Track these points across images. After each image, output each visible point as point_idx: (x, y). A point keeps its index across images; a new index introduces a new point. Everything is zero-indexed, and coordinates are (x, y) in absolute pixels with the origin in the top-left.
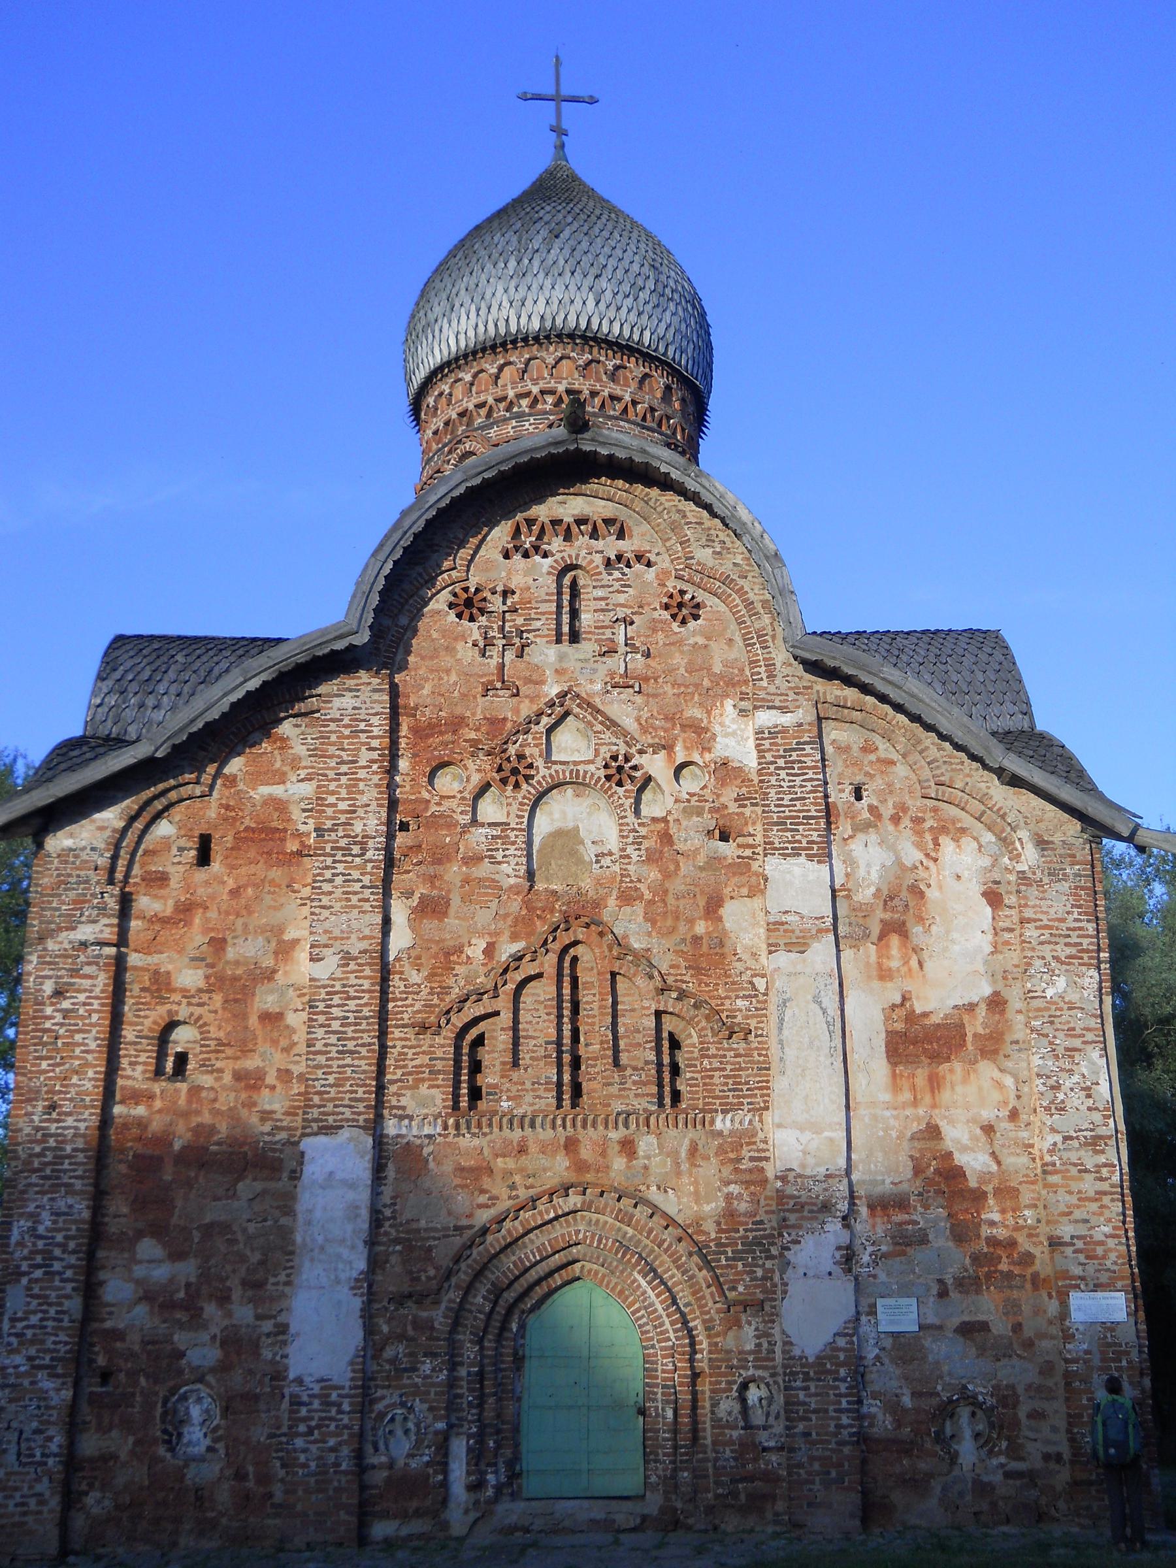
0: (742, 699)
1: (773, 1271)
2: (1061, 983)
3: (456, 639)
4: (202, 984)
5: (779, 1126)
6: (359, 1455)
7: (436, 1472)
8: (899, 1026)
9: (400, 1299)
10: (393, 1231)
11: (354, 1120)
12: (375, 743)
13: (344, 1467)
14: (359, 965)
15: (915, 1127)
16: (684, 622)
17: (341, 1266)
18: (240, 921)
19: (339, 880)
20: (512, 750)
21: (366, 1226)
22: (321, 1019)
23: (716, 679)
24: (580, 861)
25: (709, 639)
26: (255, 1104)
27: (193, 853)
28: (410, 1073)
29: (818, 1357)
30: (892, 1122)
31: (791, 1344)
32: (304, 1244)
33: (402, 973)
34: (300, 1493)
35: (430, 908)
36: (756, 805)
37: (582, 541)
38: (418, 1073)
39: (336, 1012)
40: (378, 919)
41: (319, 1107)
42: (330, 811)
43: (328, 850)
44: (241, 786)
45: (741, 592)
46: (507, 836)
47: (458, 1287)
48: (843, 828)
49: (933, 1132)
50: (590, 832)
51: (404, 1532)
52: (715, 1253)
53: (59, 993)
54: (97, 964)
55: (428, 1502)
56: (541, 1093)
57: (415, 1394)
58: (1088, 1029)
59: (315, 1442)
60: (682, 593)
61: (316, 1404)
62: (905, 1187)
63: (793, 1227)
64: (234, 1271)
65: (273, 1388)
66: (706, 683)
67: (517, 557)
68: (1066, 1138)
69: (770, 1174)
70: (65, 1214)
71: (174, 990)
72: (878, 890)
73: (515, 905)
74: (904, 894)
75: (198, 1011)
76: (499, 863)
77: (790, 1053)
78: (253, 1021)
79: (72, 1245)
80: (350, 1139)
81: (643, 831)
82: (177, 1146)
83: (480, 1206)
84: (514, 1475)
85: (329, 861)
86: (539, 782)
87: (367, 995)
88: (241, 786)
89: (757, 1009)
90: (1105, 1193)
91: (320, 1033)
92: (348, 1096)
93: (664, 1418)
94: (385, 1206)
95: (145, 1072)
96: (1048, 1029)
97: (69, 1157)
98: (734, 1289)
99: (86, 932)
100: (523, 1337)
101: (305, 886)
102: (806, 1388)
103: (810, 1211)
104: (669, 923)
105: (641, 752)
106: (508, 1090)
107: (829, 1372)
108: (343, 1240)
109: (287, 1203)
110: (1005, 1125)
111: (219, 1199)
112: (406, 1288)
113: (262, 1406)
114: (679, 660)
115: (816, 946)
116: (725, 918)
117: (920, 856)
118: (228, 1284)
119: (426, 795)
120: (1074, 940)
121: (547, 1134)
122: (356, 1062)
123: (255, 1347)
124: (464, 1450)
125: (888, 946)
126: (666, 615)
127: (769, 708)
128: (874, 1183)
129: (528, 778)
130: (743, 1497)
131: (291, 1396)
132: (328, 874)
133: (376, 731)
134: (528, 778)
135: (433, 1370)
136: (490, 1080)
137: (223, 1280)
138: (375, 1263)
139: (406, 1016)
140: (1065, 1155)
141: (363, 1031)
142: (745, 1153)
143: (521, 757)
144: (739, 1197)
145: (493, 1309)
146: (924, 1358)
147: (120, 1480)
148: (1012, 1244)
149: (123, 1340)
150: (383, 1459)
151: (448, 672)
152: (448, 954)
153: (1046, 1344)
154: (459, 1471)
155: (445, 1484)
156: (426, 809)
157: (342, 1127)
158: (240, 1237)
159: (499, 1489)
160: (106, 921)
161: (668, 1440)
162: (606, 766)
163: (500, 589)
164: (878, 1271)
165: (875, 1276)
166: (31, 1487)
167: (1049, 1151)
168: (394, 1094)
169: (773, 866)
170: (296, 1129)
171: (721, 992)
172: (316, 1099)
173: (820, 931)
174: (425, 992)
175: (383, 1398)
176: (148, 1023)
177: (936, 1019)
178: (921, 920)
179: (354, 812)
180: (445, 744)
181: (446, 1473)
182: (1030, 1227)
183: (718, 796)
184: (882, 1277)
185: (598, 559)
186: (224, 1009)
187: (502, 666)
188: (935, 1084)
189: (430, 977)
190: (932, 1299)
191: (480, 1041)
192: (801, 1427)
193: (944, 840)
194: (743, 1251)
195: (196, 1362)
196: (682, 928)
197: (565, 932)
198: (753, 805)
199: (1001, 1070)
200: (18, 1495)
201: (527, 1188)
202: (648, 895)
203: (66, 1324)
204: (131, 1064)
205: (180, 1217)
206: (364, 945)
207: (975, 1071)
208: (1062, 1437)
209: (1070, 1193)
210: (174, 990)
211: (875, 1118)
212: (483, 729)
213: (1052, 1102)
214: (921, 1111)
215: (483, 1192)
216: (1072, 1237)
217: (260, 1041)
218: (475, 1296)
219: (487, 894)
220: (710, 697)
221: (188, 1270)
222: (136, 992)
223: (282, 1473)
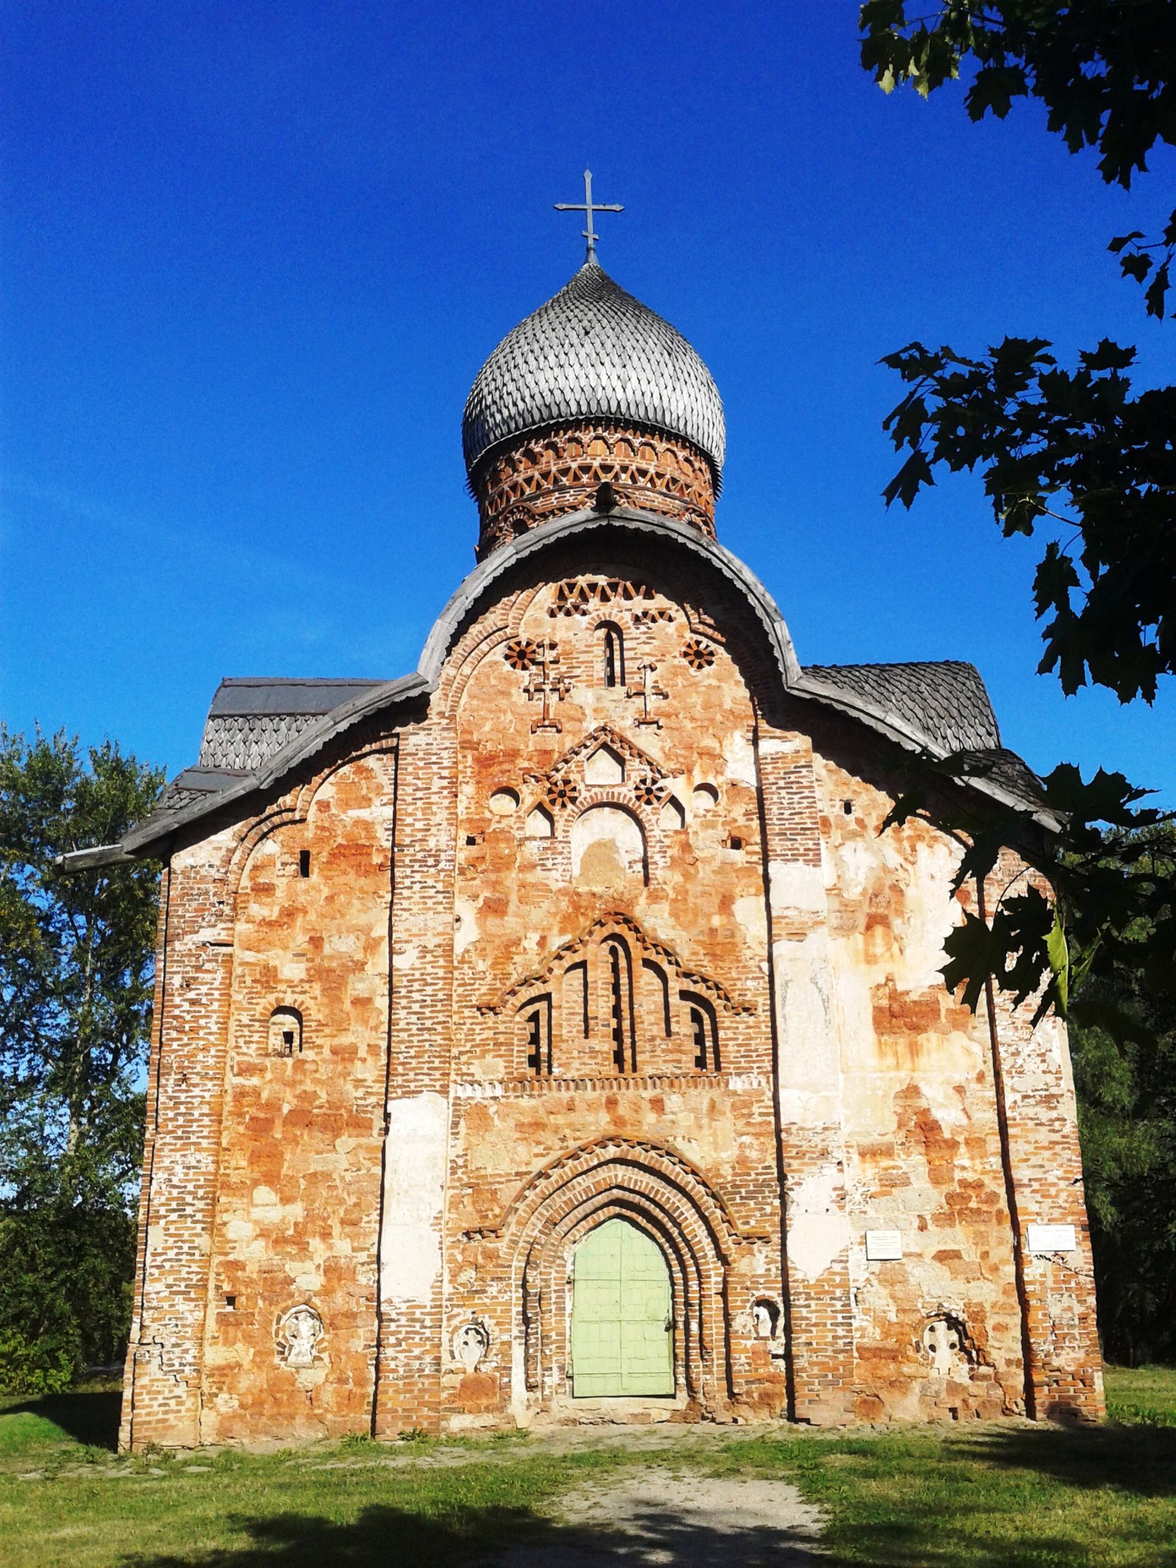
4: (304, 976)
8: (885, 1003)
10: (465, 1177)
12: (445, 773)
13: (427, 1372)
15: (898, 1088)
16: (700, 667)
19: (417, 887)
20: (558, 777)
22: (404, 1002)
24: (616, 867)
25: (720, 680)
27: (294, 867)
30: (879, 1083)
34: (391, 1393)
35: (494, 908)
39: (416, 996)
40: (450, 918)
42: (408, 830)
43: (407, 862)
44: (334, 810)
48: (836, 836)
49: (912, 1091)
51: (477, 1425)
53: (187, 985)
56: (586, 1060)
59: (404, 1351)
61: (403, 1320)
62: (890, 1138)
66: (719, 718)
67: (561, 615)
71: (281, 981)
72: (865, 890)
73: (564, 904)
74: (887, 891)
75: (300, 998)
81: (667, 842)
82: (286, 1109)
83: (536, 1155)
85: (408, 871)
98: (747, 1223)
99: (207, 935)
102: (808, 1306)
105: (663, 777)
107: (826, 1292)
112: (477, 1224)
113: (359, 1322)
114: (696, 699)
115: (812, 936)
117: (901, 860)
119: (488, 815)
121: (590, 1094)
125: (873, 936)
129: (573, 800)
130: (756, 1395)
132: (407, 882)
134: (573, 800)
139: (474, 998)
140: (1024, 1111)
143: (567, 782)
144: (751, 1146)
146: (905, 1282)
147: (244, 1383)
148: (979, 1185)
149: (244, 1269)
150: (459, 1365)
151: (505, 712)
152: (507, 946)
158: (338, 1182)
160: (224, 925)
162: (637, 788)
163: (547, 642)
166: (171, 1391)
171: (734, 975)
172: (400, 1069)
173: (816, 923)
174: (489, 978)
176: (259, 1008)
177: (914, 996)
178: (900, 913)
180: (503, 772)
181: (509, 1375)
185: (627, 617)
186: (323, 995)
187: (546, 708)
188: (914, 1050)
189: (494, 965)
191: (534, 1018)
192: (803, 1338)
193: (921, 847)
196: (702, 922)
200: (160, 1397)
201: (575, 1139)
202: (672, 895)
203: (197, 1257)
209: (1028, 1142)
210: (281, 981)
215: (538, 1143)
221: (296, 1211)
222: (248, 980)
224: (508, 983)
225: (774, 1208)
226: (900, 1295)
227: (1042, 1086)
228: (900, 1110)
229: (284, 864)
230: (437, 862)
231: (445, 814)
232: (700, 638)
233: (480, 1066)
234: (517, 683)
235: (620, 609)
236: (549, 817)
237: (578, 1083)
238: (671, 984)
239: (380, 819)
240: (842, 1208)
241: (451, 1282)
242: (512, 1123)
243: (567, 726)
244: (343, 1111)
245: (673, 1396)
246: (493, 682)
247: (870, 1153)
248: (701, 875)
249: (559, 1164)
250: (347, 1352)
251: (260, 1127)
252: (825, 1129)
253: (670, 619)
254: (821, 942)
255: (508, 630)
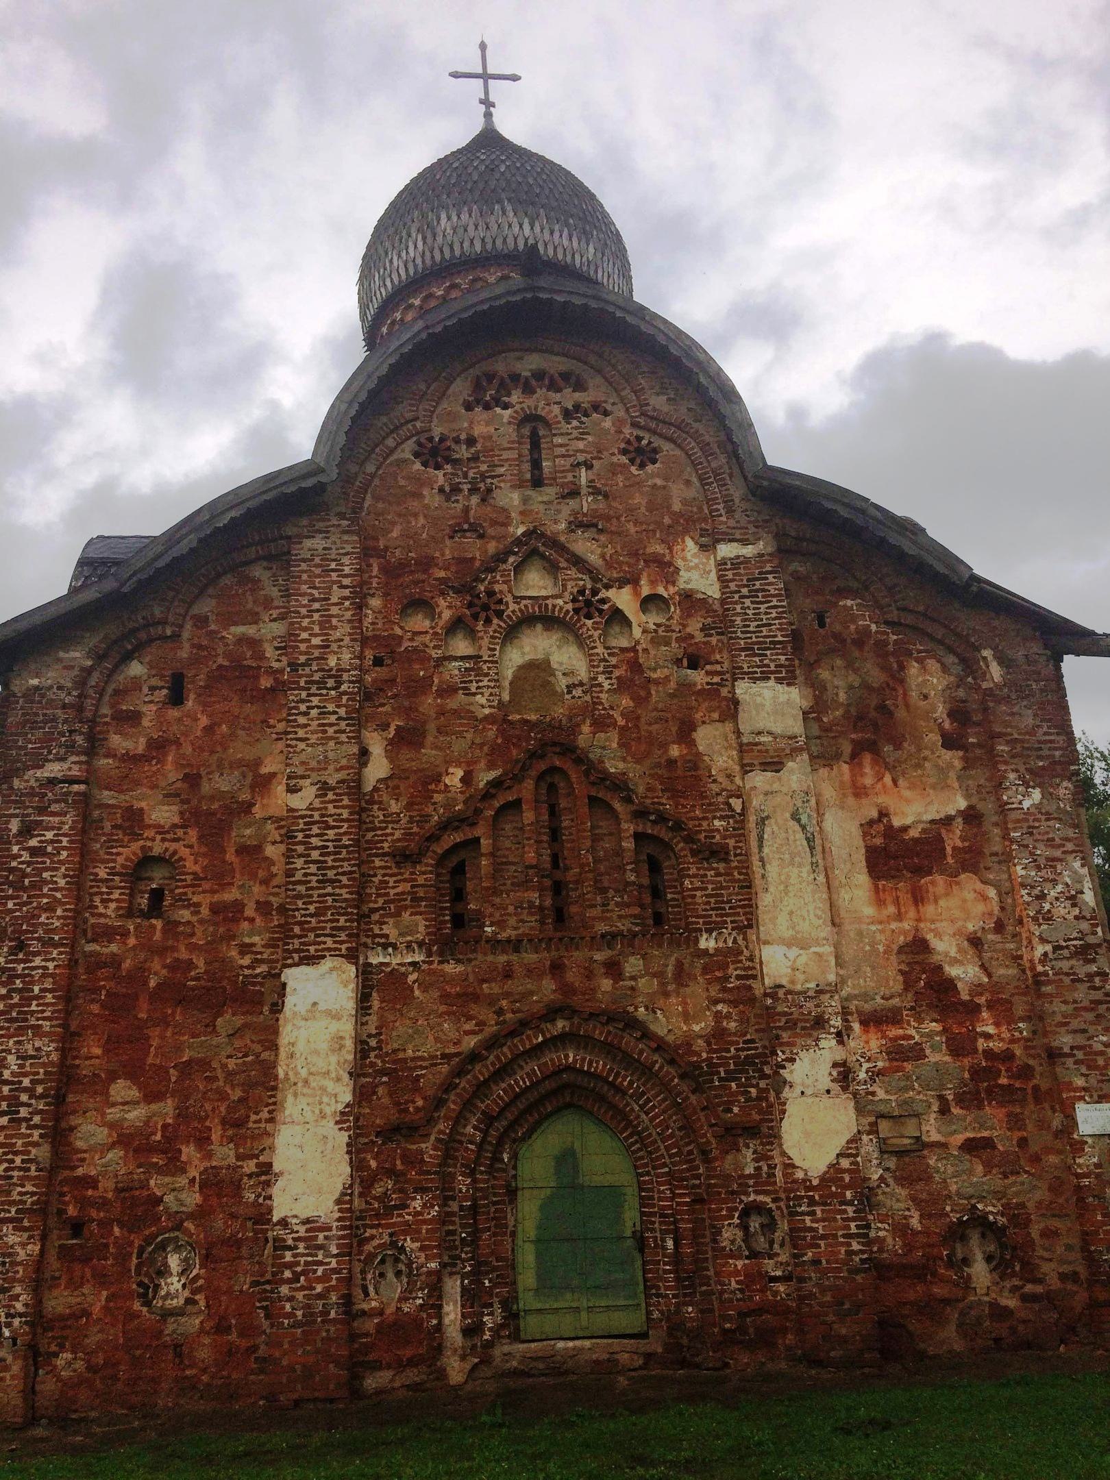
0: (702, 536)
1: (766, 1090)
2: (1036, 795)
3: (422, 485)
4: (176, 820)
5: (766, 943)
6: (348, 1300)
7: (430, 1317)
8: (878, 841)
9: (391, 1132)
10: (379, 1062)
11: (335, 949)
12: (346, 582)
14: (337, 794)
16: (642, 466)
17: (325, 1099)
18: (215, 757)
19: (314, 712)
21: (351, 1057)
22: (300, 849)
23: (677, 516)
25: (666, 479)
26: (233, 937)
27: (165, 692)
28: (392, 901)
29: (823, 1178)
30: (879, 937)
31: (793, 1166)
32: (287, 1078)
33: (381, 803)
35: (406, 739)
36: (722, 634)
37: (540, 392)
38: (400, 900)
40: (355, 749)
41: (300, 937)
42: (303, 647)
43: (302, 684)
45: (696, 436)
46: (480, 668)
47: (447, 1118)
49: (918, 946)
50: (561, 664)
52: (707, 1073)
54: (66, 801)
55: (422, 1351)
57: (405, 1233)
58: (1068, 839)
59: (302, 1288)
60: (639, 439)
62: (896, 1001)
63: (789, 1044)
64: (213, 1110)
65: (256, 1232)
68: (1057, 948)
69: (758, 992)
70: (32, 1057)
71: (149, 826)
72: (847, 712)
73: (492, 731)
74: (873, 714)
75: (173, 846)
76: (474, 694)
77: (773, 870)
78: (230, 856)
79: (40, 1089)
80: (332, 970)
81: (614, 660)
83: (467, 1033)
84: (512, 1316)
85: (304, 694)
86: (509, 616)
87: (346, 825)
88: (213, 627)
89: (734, 829)
90: (1099, 1002)
91: (299, 863)
92: (329, 925)
93: (664, 1248)
94: (370, 1036)
95: (118, 908)
96: (1028, 840)
97: (37, 998)
99: (54, 769)
100: (515, 1168)
101: (279, 721)
102: (813, 1213)
103: (803, 1028)
104: (643, 747)
105: (607, 587)
106: (491, 915)
107: (833, 1195)
108: (328, 1072)
109: (269, 1037)
110: (991, 937)
111: (198, 1036)
113: (245, 1251)
114: (639, 500)
116: (698, 741)
118: (207, 1124)
119: (398, 631)
120: (1045, 752)
121: (530, 957)
122: (338, 891)
123: (237, 1188)
124: (459, 1290)
125: (860, 765)
126: (624, 459)
127: (731, 541)
128: (866, 997)
129: (499, 614)
130: (751, 1330)
131: (275, 1240)
132: (303, 708)
133: (347, 570)
134: (499, 614)
135: (424, 1206)
136: (472, 906)
137: (202, 1120)
138: (363, 1094)
141: (343, 860)
142: (733, 972)
143: (490, 593)
144: (728, 1016)
145: (483, 1140)
148: (1008, 1056)
150: (374, 1304)
151: (416, 515)
153: (1053, 1159)
154: (452, 1313)
155: (439, 1328)
156: (400, 645)
157: (324, 957)
158: (219, 1073)
159: (496, 1331)
160: (74, 758)
161: (669, 1272)
162: (574, 600)
163: (463, 436)
164: (875, 1088)
165: (873, 1094)
167: (1040, 961)
168: (377, 922)
169: (743, 689)
170: (277, 961)
172: (297, 930)
175: (373, 1237)
176: (120, 860)
177: (914, 833)
179: (328, 647)
181: (440, 1317)
182: (1027, 1040)
183: (684, 626)
184: (881, 1094)
185: (556, 410)
187: (466, 510)
188: (918, 898)
189: (409, 806)
190: (933, 1116)
191: (459, 870)
194: (735, 1071)
195: (174, 1208)
197: (543, 756)
198: (718, 634)
199: (982, 882)
201: (514, 1012)
202: (621, 722)
204: (103, 901)
205: (156, 1055)
206: (342, 775)
207: (958, 883)
208: (1076, 1255)
211: (860, 933)
212: (453, 569)
213: (1038, 912)
214: (906, 925)
216: (1072, 1048)
217: (238, 876)
218: (465, 1126)
219: (461, 725)
220: (671, 535)
222: (108, 826)
223: (265, 1324)
224: (427, 826)
225: (760, 1091)
226: (924, 1196)
227: (1075, 935)
228: (904, 967)
229: (153, 689)
230: (339, 684)
231: (347, 628)
232: (641, 434)
233: (396, 925)
234: (430, 483)
235: (549, 404)
236: (472, 635)
237: (515, 945)
238: (625, 826)
239: (269, 637)
240: (845, 1089)
241: (361, 1195)
242: (436, 994)
243: (491, 531)
244: (225, 983)
245: (643, 1336)
246: (402, 482)
247: (873, 1020)
248: (654, 698)
249: (492, 1044)
250: (229, 1291)
251: (119, 1006)
252: (820, 992)
253: (606, 413)
254: (796, 774)
255: (418, 424)
